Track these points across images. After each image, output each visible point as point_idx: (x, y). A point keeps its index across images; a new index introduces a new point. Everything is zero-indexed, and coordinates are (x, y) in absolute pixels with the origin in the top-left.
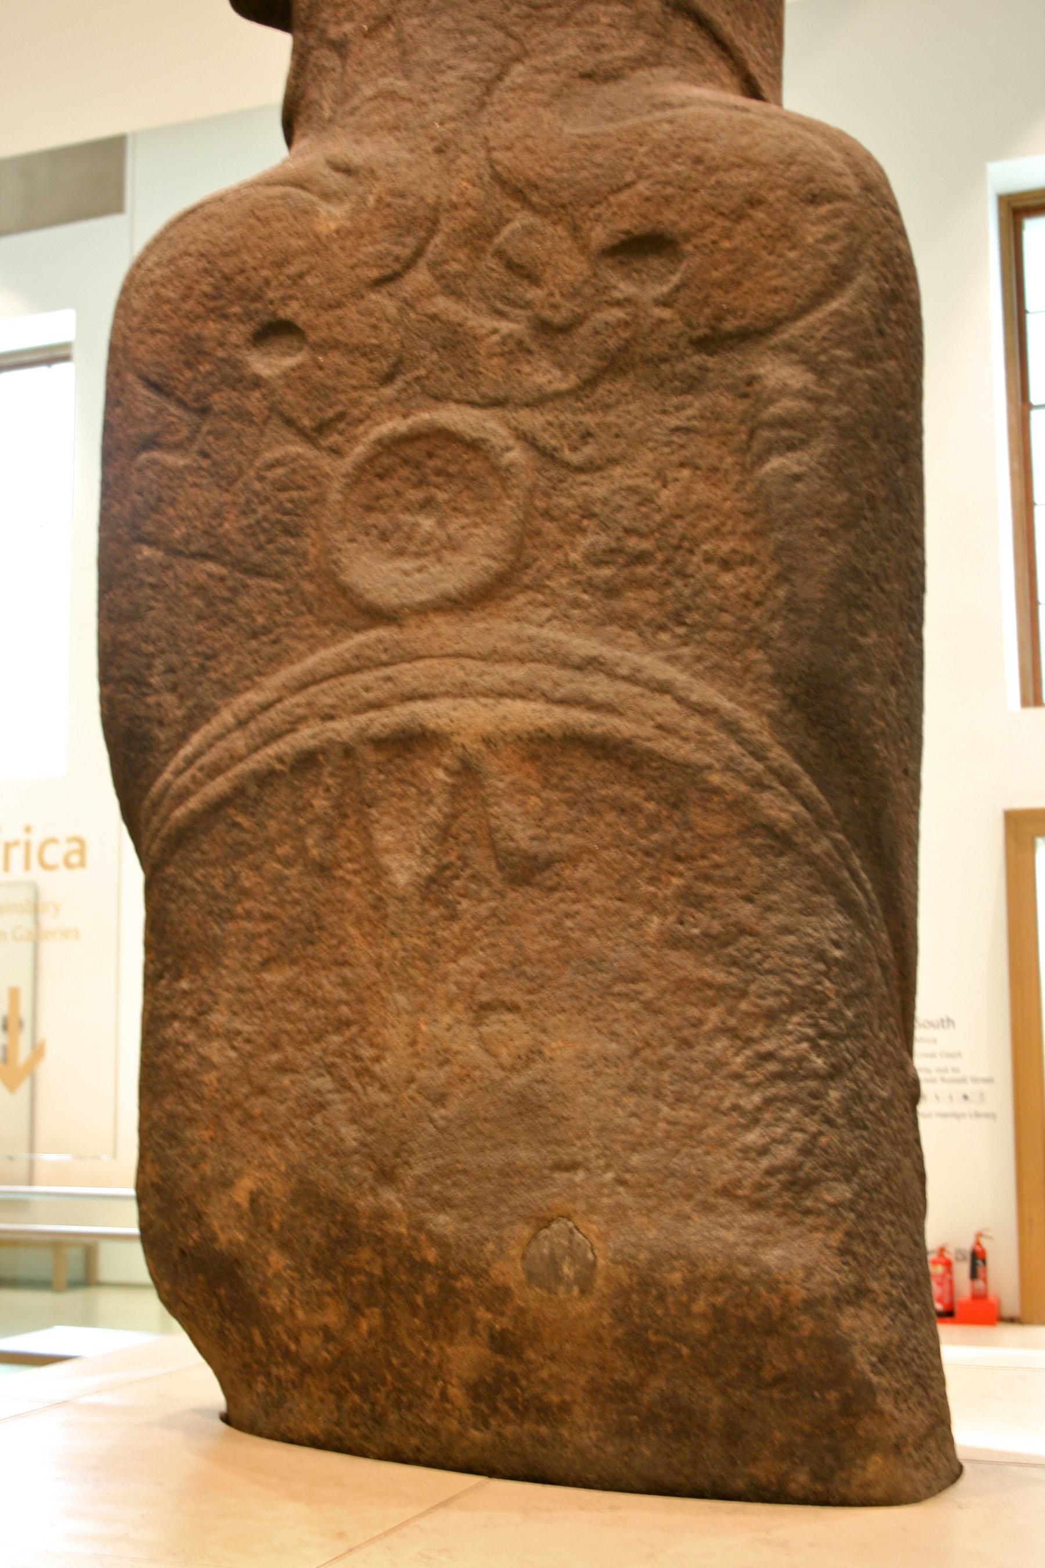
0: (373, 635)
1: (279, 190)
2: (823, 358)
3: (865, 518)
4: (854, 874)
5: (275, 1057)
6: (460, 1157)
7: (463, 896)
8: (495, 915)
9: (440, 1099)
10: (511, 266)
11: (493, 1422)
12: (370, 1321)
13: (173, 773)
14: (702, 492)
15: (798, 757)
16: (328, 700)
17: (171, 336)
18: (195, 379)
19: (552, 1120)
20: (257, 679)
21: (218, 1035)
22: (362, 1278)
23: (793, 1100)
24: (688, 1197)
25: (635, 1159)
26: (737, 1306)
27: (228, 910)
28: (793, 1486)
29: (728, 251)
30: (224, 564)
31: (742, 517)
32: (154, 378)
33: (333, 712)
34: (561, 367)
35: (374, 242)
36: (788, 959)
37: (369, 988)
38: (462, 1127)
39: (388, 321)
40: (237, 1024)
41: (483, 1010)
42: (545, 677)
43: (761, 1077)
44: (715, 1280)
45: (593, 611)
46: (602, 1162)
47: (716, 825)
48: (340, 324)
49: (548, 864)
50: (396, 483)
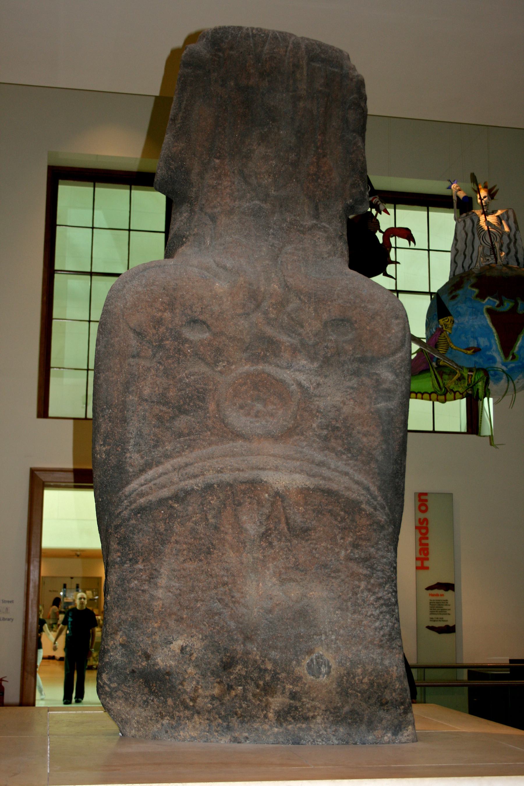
11: (284, 725)
13: (137, 484)
24: (360, 644)
40: (173, 583)
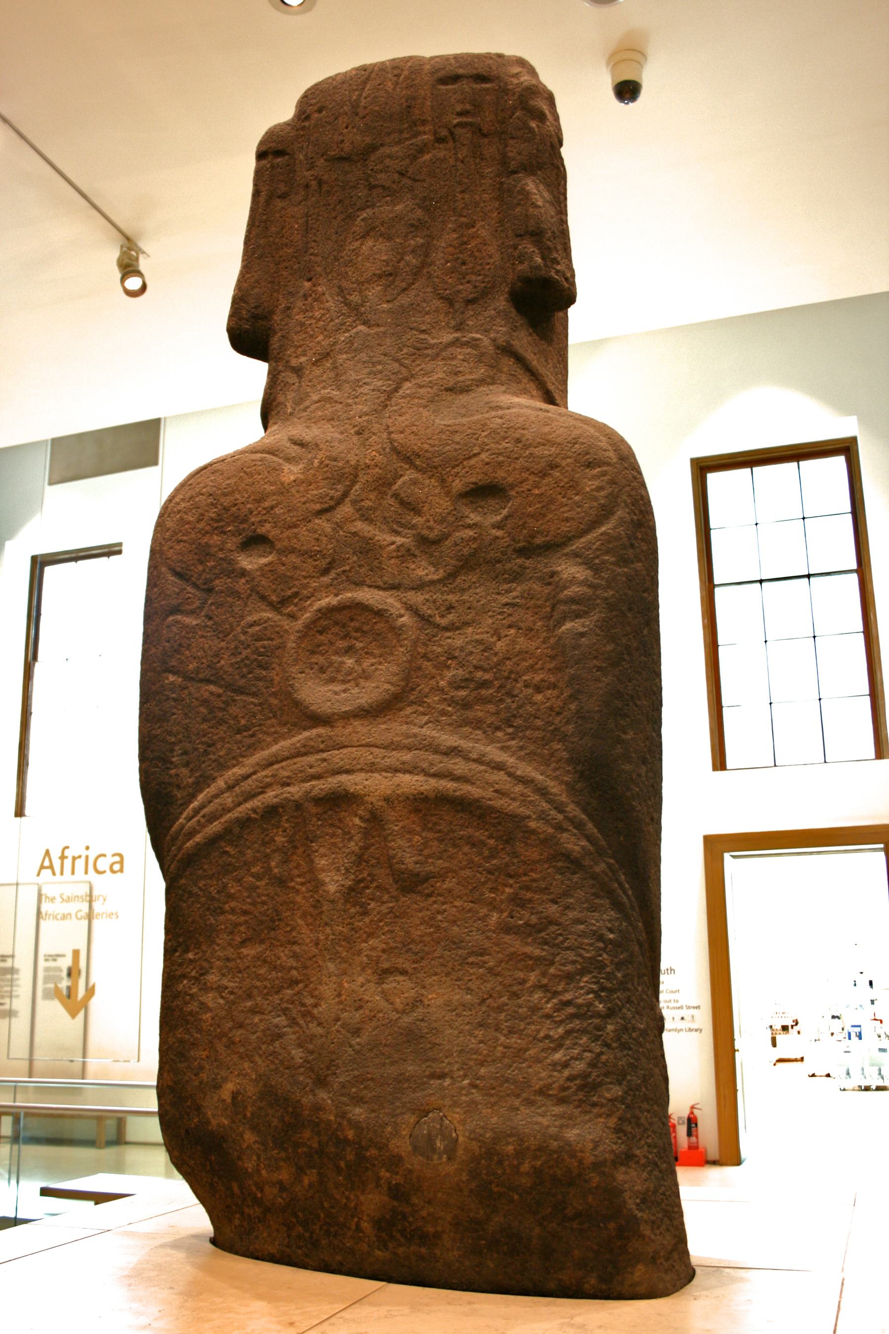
0: (314, 732)
1: (259, 455)
2: (597, 561)
3: (625, 660)
4: (621, 885)
5: (249, 1004)
6: (370, 1070)
7: (372, 900)
8: (391, 912)
9: (357, 1032)
10: (402, 503)
11: (390, 1245)
12: (310, 1177)
13: (185, 818)
14: (523, 643)
15: (584, 811)
16: (286, 774)
17: (189, 543)
18: (204, 571)
19: (429, 1046)
20: (241, 759)
21: (212, 989)
22: (305, 1149)
23: (584, 1031)
24: (518, 1096)
25: (483, 1071)
26: (549, 1167)
27: (221, 908)
28: (586, 1286)
29: (537, 495)
30: (221, 687)
31: (548, 659)
32: (178, 569)
33: (288, 781)
34: (434, 566)
35: (317, 488)
36: (579, 940)
37: (310, 959)
38: (371, 1050)
39: (326, 536)
40: (225, 982)
41: (385, 973)
42: (424, 760)
43: (563, 1017)
44: (535, 1150)
45: (454, 717)
46: (461, 1073)
47: (534, 854)
48: (296, 538)
49: (426, 879)
50: (330, 636)
